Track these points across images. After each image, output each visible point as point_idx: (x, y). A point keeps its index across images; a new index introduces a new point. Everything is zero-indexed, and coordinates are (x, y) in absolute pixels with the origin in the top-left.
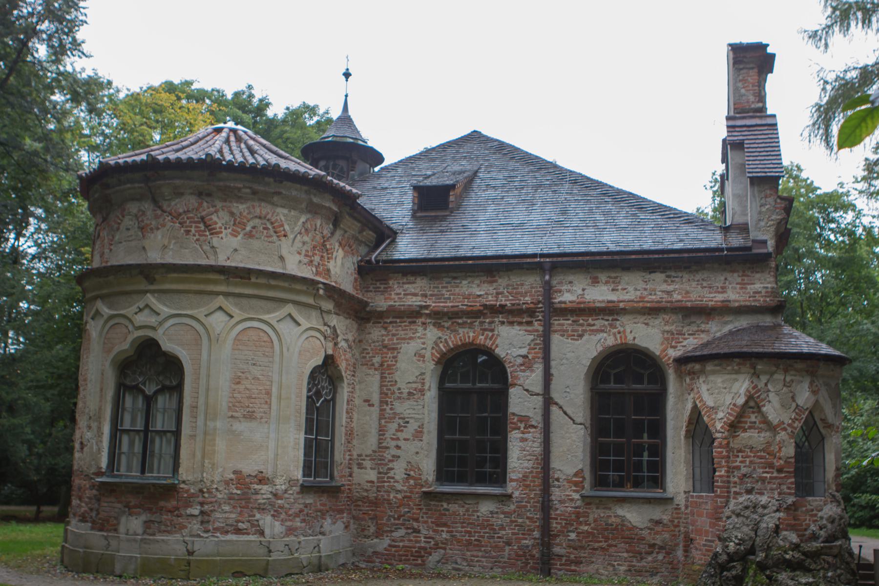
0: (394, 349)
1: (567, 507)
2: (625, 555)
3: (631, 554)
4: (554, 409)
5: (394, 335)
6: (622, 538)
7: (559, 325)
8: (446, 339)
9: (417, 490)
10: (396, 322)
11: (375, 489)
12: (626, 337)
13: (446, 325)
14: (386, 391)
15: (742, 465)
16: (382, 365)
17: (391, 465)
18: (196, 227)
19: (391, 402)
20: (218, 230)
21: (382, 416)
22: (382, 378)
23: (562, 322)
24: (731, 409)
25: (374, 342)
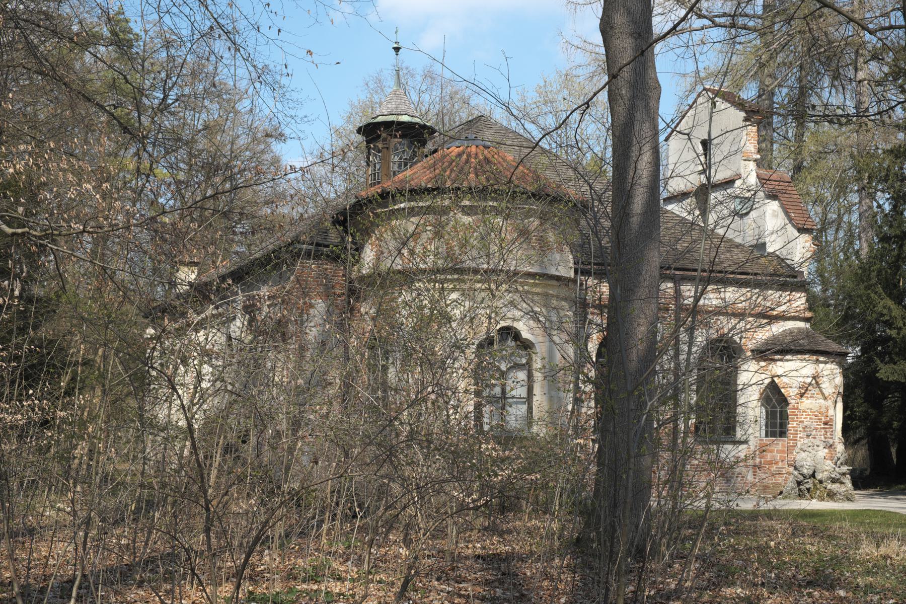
15: (805, 420)
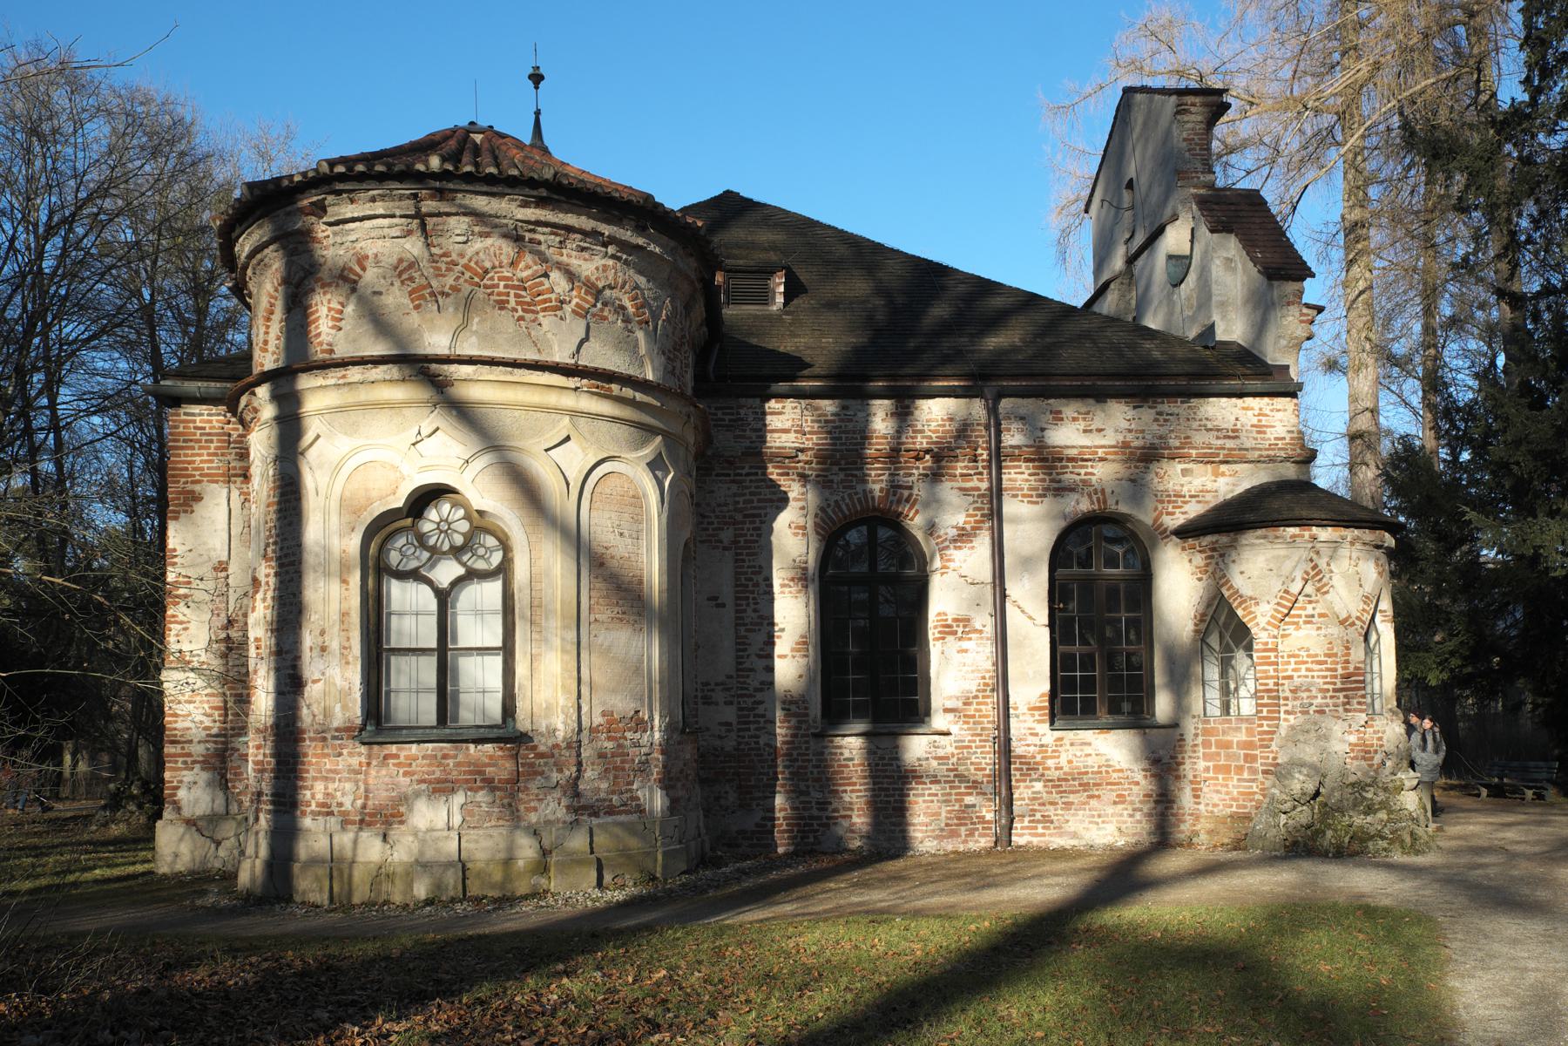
0: (754, 516)
1: (1028, 745)
2: (1110, 810)
3: (1120, 807)
4: (1008, 605)
5: (751, 494)
6: (1108, 784)
7: (1010, 480)
8: (836, 502)
9: (802, 732)
10: (757, 474)
11: (733, 735)
12: (1105, 502)
13: (835, 478)
14: (744, 582)
15: (1295, 674)
16: (735, 542)
17: (759, 696)
18: (517, 296)
19: (754, 599)
20: (554, 303)
21: (739, 622)
22: (736, 561)
23: (1013, 476)
24: (1281, 598)
25: (719, 505)
